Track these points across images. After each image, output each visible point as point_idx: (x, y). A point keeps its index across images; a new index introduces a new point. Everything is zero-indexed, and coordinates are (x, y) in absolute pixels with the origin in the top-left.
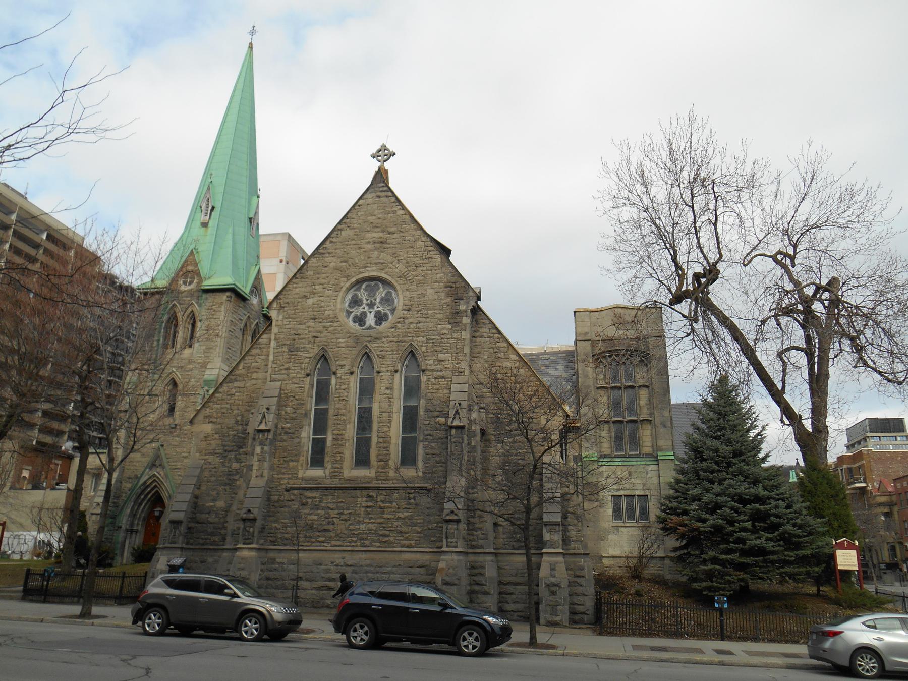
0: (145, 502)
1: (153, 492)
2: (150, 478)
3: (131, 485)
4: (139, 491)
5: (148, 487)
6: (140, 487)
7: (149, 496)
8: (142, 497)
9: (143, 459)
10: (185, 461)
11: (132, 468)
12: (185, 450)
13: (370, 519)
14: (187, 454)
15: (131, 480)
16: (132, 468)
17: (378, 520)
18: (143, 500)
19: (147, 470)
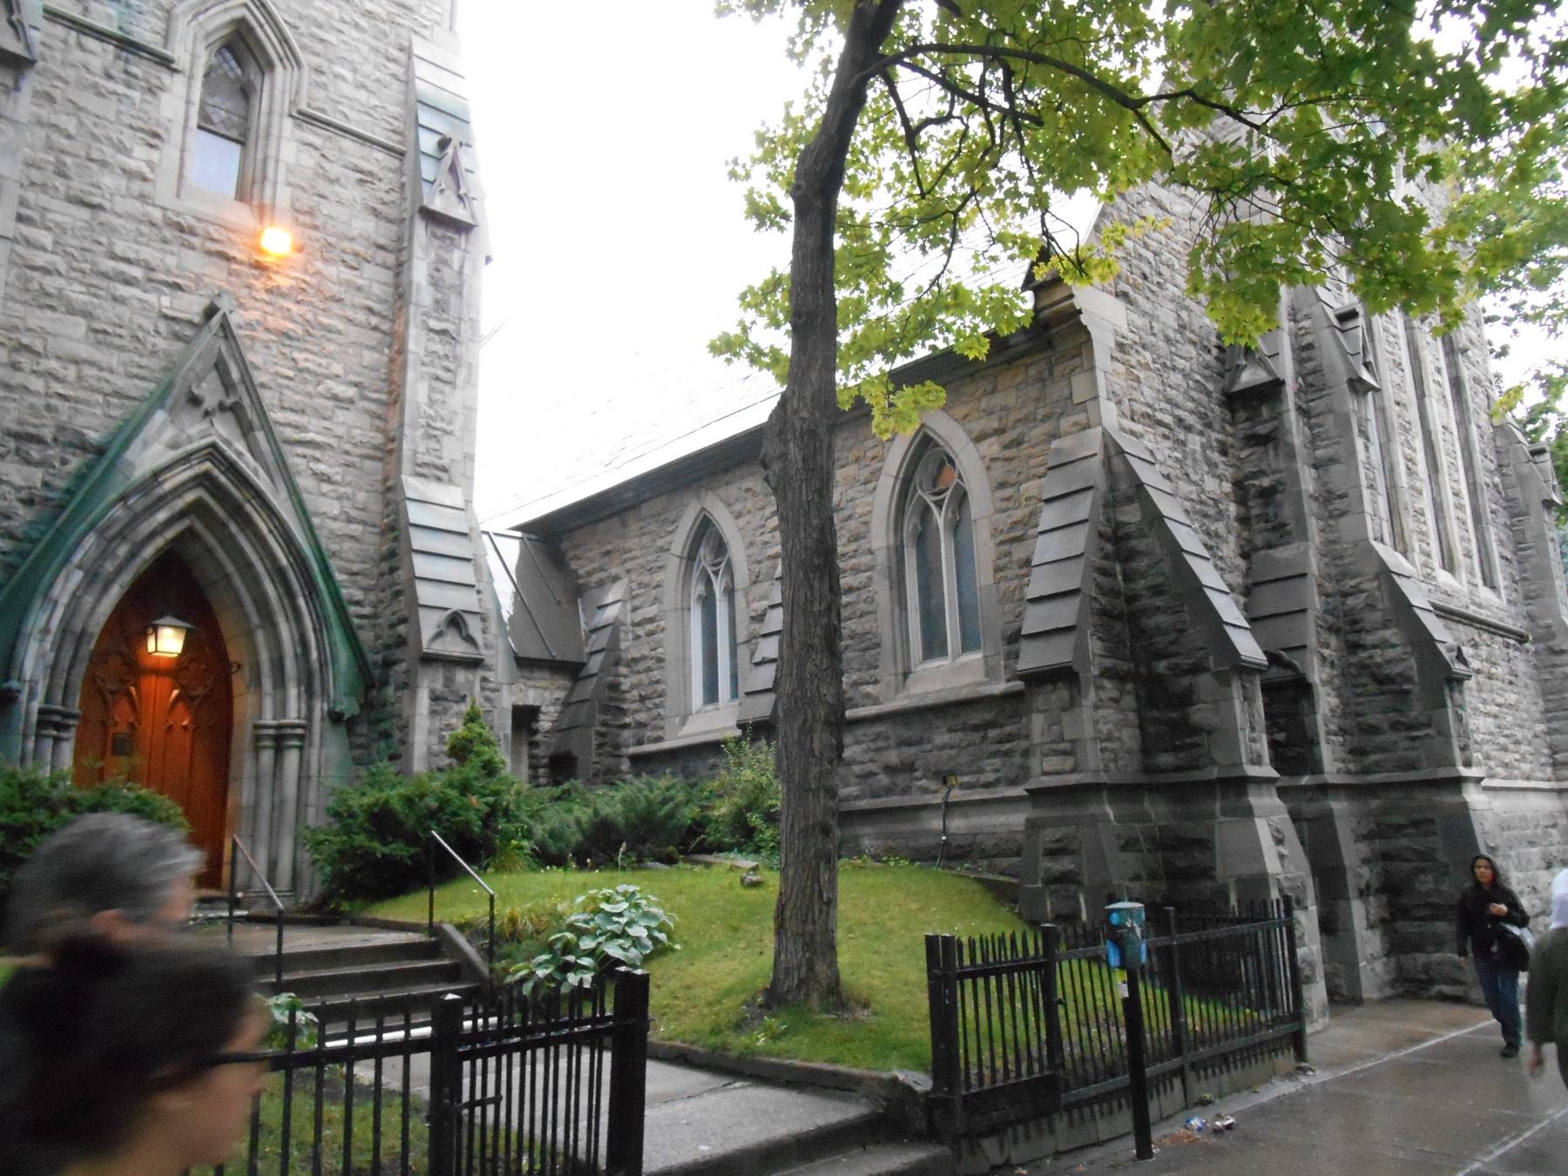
0: (127, 578)
1: (170, 534)
2: (186, 459)
3: (37, 475)
4: (118, 511)
5: (162, 501)
6: (123, 498)
7: (149, 552)
8: (123, 550)
9: (112, 359)
10: (341, 416)
11: (37, 384)
12: (337, 368)
13: (1484, 702)
14: (351, 392)
15: (35, 452)
16: (37, 384)
17: (1495, 709)
18: (120, 570)
19: (160, 416)
